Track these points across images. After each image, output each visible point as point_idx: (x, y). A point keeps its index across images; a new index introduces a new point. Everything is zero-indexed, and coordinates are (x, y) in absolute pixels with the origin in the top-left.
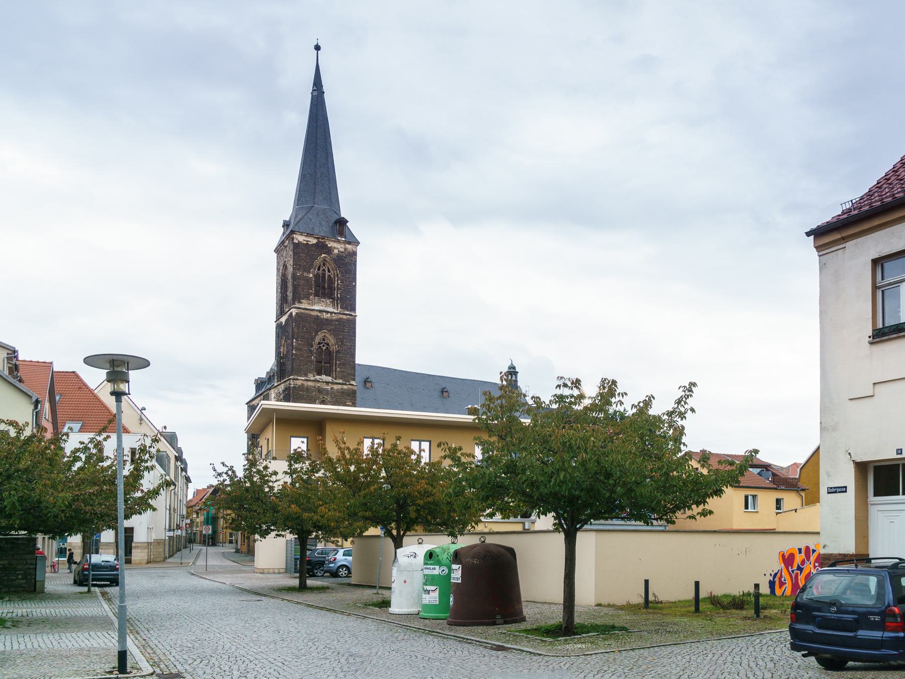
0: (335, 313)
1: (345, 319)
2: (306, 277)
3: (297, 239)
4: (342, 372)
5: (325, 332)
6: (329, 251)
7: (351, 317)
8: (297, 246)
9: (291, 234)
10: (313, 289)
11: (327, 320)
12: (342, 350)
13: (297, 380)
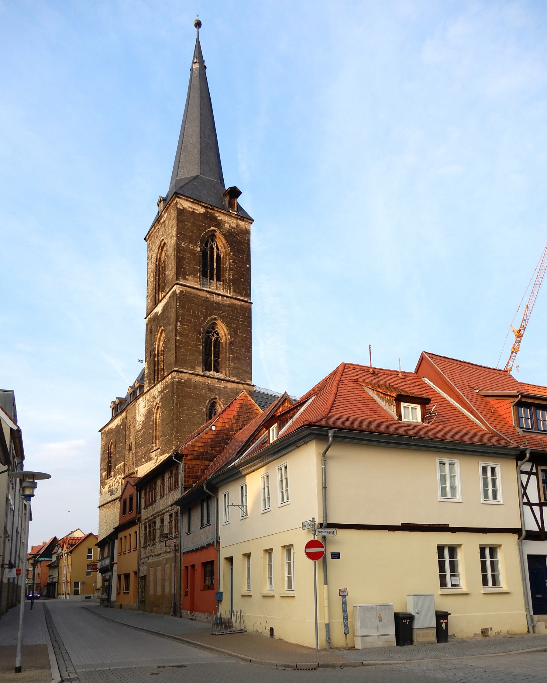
0: (227, 297)
1: (238, 305)
2: (193, 250)
3: (181, 204)
4: (238, 368)
6: (219, 224)
7: (245, 304)
9: (174, 199)
11: (218, 303)
13: (184, 373)
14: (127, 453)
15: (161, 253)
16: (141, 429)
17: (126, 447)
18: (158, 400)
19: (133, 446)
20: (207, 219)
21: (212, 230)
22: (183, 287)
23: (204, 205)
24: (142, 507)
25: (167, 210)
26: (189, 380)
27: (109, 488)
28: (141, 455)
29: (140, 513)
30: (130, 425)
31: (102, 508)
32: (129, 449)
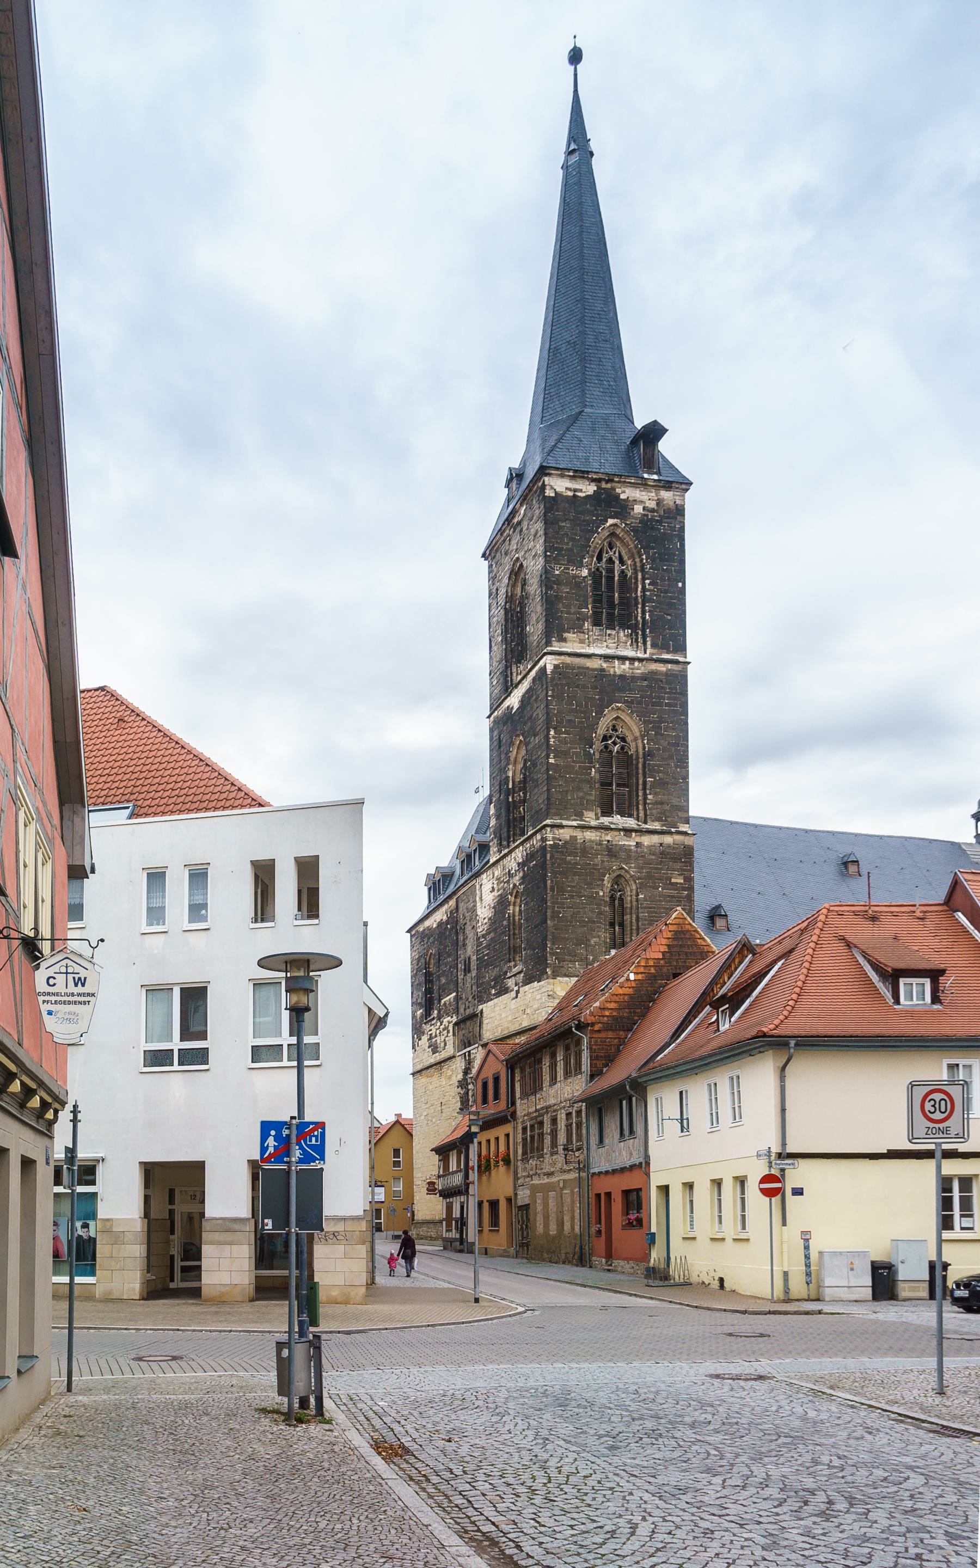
0: (641, 660)
2: (575, 577)
3: (552, 488)
5: (619, 709)
6: (622, 509)
8: (553, 504)
9: (539, 480)
10: (590, 607)
11: (622, 677)
12: (658, 749)
15: (514, 586)
16: (488, 933)
17: (460, 965)
18: (516, 880)
19: (472, 964)
20: (600, 506)
21: (611, 526)
22: (557, 657)
23: (594, 477)
24: (518, 1094)
25: (524, 500)
26: (574, 838)
28: (489, 983)
29: (513, 1103)
30: (466, 924)
32: (465, 969)
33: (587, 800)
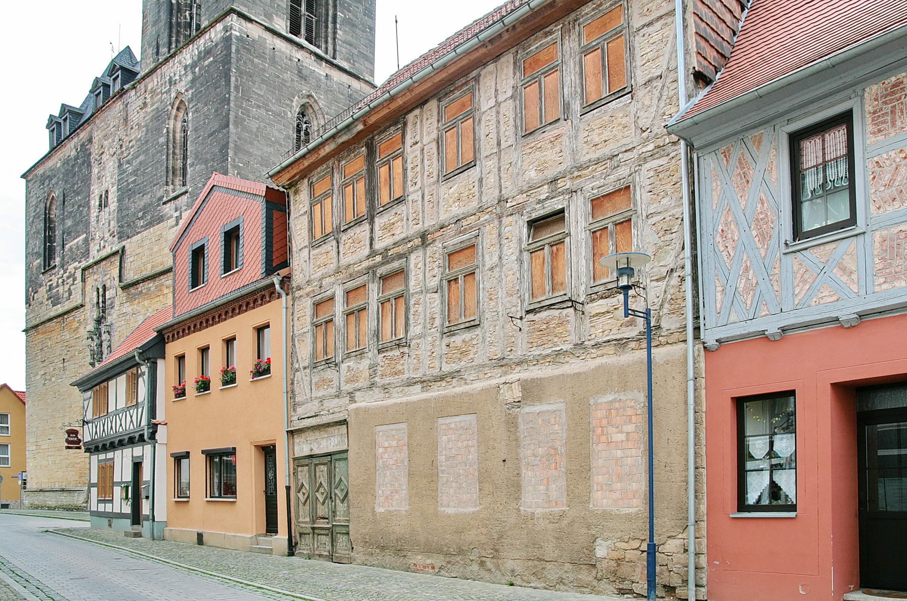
14: (94, 213)
27: (47, 291)
31: (32, 332)
33: (278, 5)
